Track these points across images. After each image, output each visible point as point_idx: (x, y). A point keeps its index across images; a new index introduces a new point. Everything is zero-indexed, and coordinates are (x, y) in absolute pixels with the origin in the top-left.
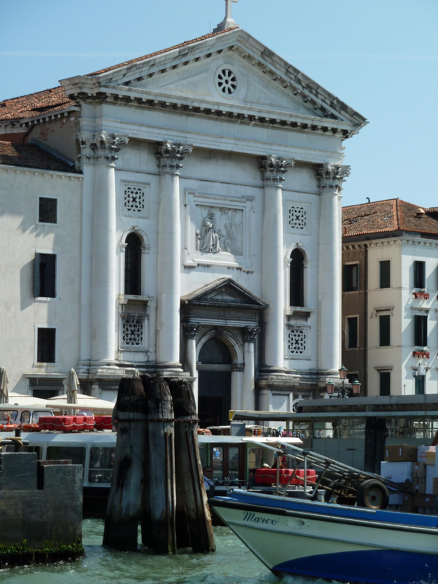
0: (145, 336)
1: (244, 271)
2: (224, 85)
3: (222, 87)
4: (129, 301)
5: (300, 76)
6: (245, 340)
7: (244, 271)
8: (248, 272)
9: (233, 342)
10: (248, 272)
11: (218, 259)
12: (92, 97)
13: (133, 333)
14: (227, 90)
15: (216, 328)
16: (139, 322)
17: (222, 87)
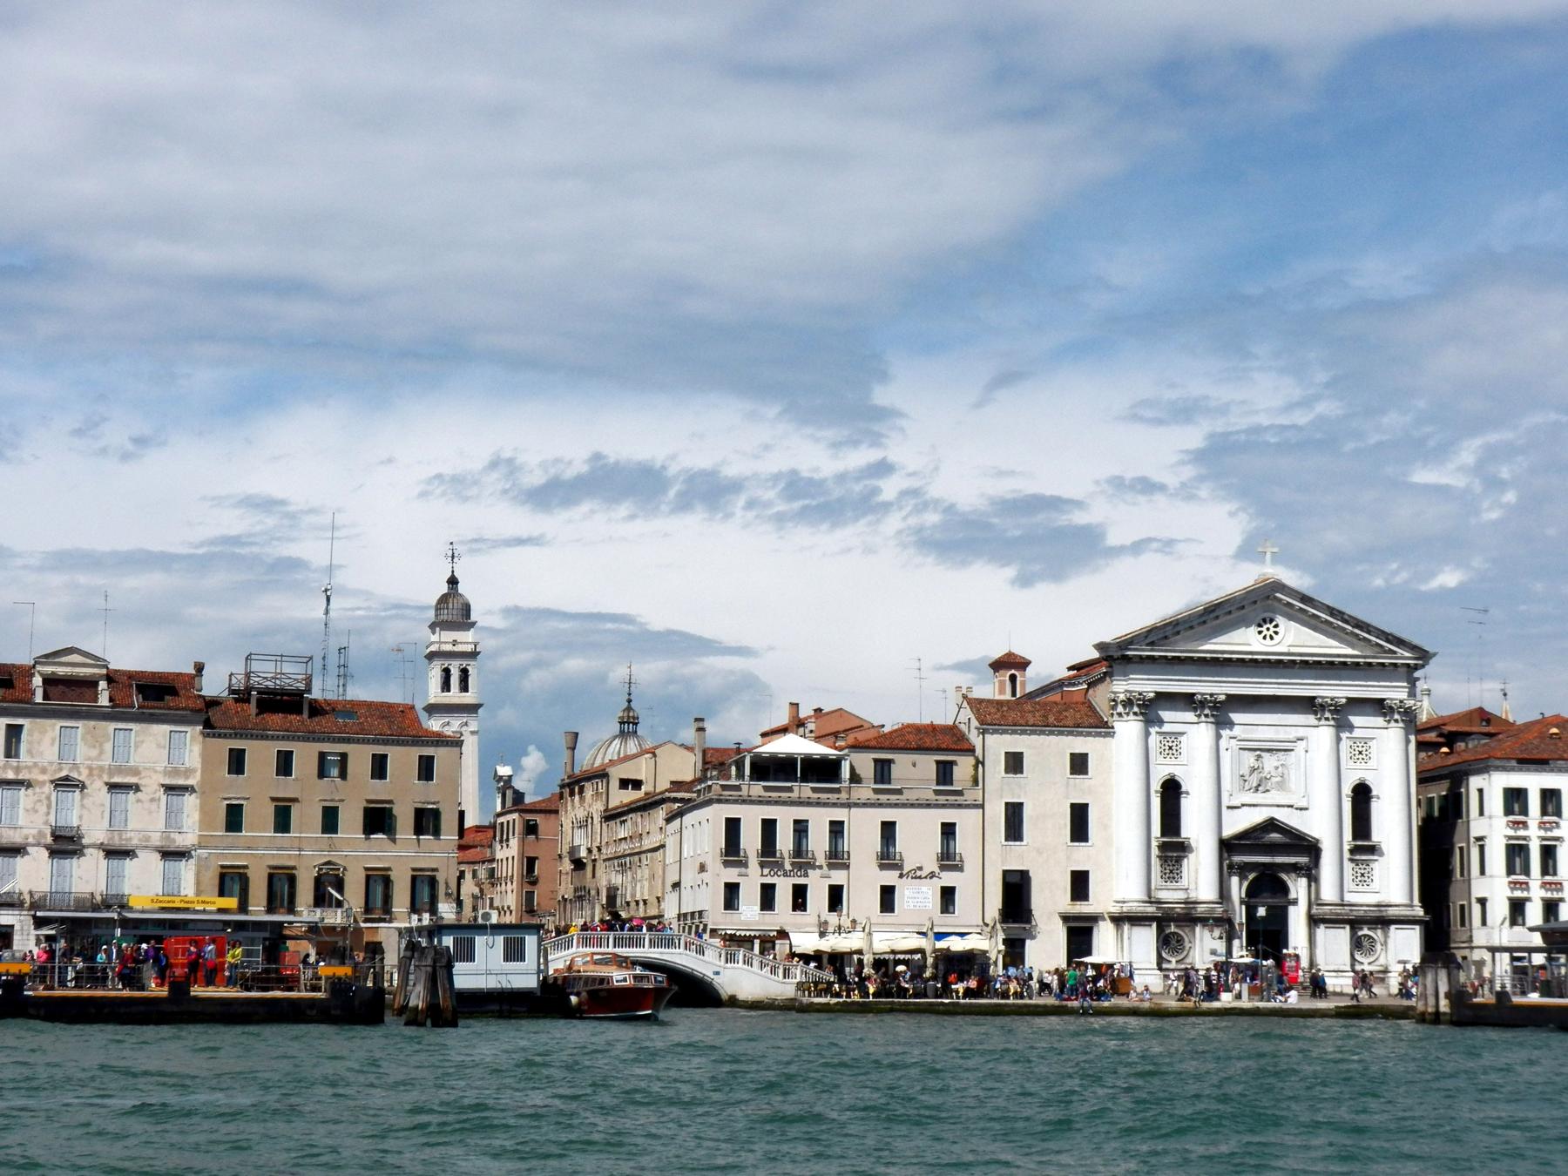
0: (1185, 874)
1: (1297, 809)
2: (1265, 632)
3: (1263, 634)
4: (1164, 842)
5: (1346, 617)
6: (1299, 876)
7: (1297, 809)
8: (1301, 809)
9: (1284, 876)
10: (1301, 809)
11: (1265, 798)
12: (1118, 658)
13: (1171, 872)
14: (1268, 637)
15: (1264, 864)
16: (1179, 860)
17: (1263, 634)
